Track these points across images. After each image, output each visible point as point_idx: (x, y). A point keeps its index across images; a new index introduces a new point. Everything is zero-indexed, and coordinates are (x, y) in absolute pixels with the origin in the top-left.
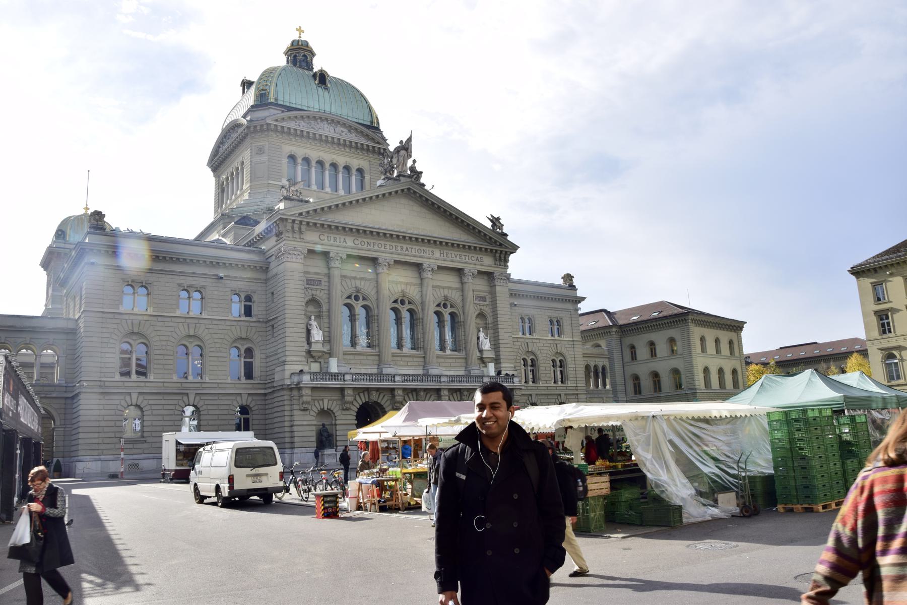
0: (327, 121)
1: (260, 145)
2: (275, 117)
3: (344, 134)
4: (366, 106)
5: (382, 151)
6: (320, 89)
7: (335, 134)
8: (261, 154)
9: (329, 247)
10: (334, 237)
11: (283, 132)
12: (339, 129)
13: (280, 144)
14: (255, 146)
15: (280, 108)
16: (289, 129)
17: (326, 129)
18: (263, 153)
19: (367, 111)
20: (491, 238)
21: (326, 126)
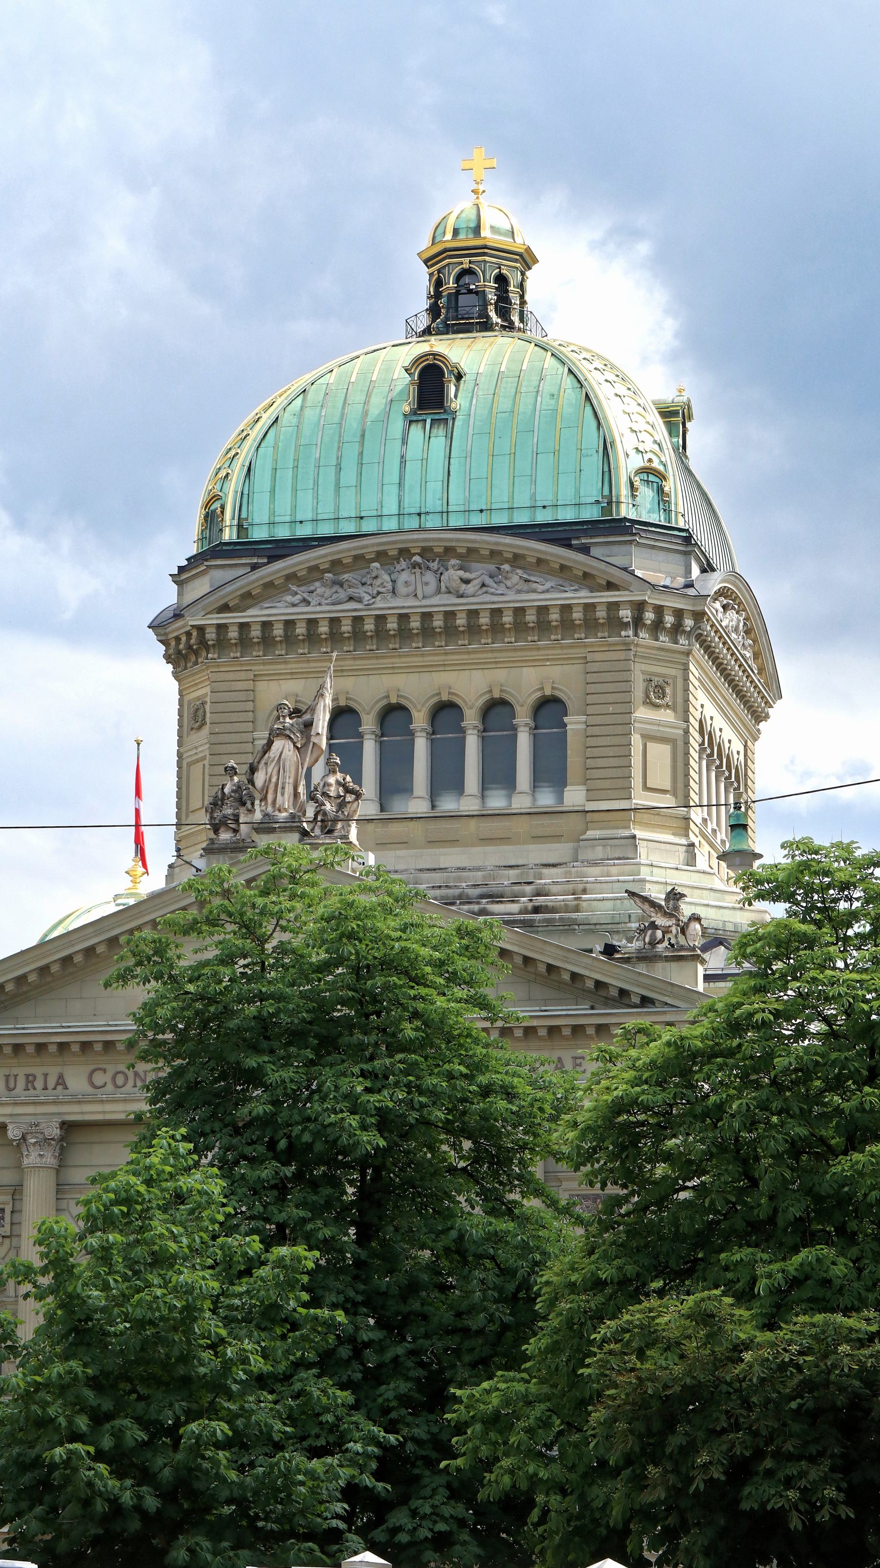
0: (410, 559)
1: (198, 698)
2: (217, 600)
3: (470, 589)
4: (596, 434)
5: (626, 614)
6: (416, 432)
7: (435, 600)
8: (200, 727)
9: (8, 1110)
10: (27, 1076)
11: (244, 642)
12: (453, 575)
13: (249, 685)
14: (189, 702)
15: (240, 557)
16: (266, 626)
17: (401, 589)
18: (203, 724)
19: (594, 463)
20: (599, 984)
21: (404, 576)
